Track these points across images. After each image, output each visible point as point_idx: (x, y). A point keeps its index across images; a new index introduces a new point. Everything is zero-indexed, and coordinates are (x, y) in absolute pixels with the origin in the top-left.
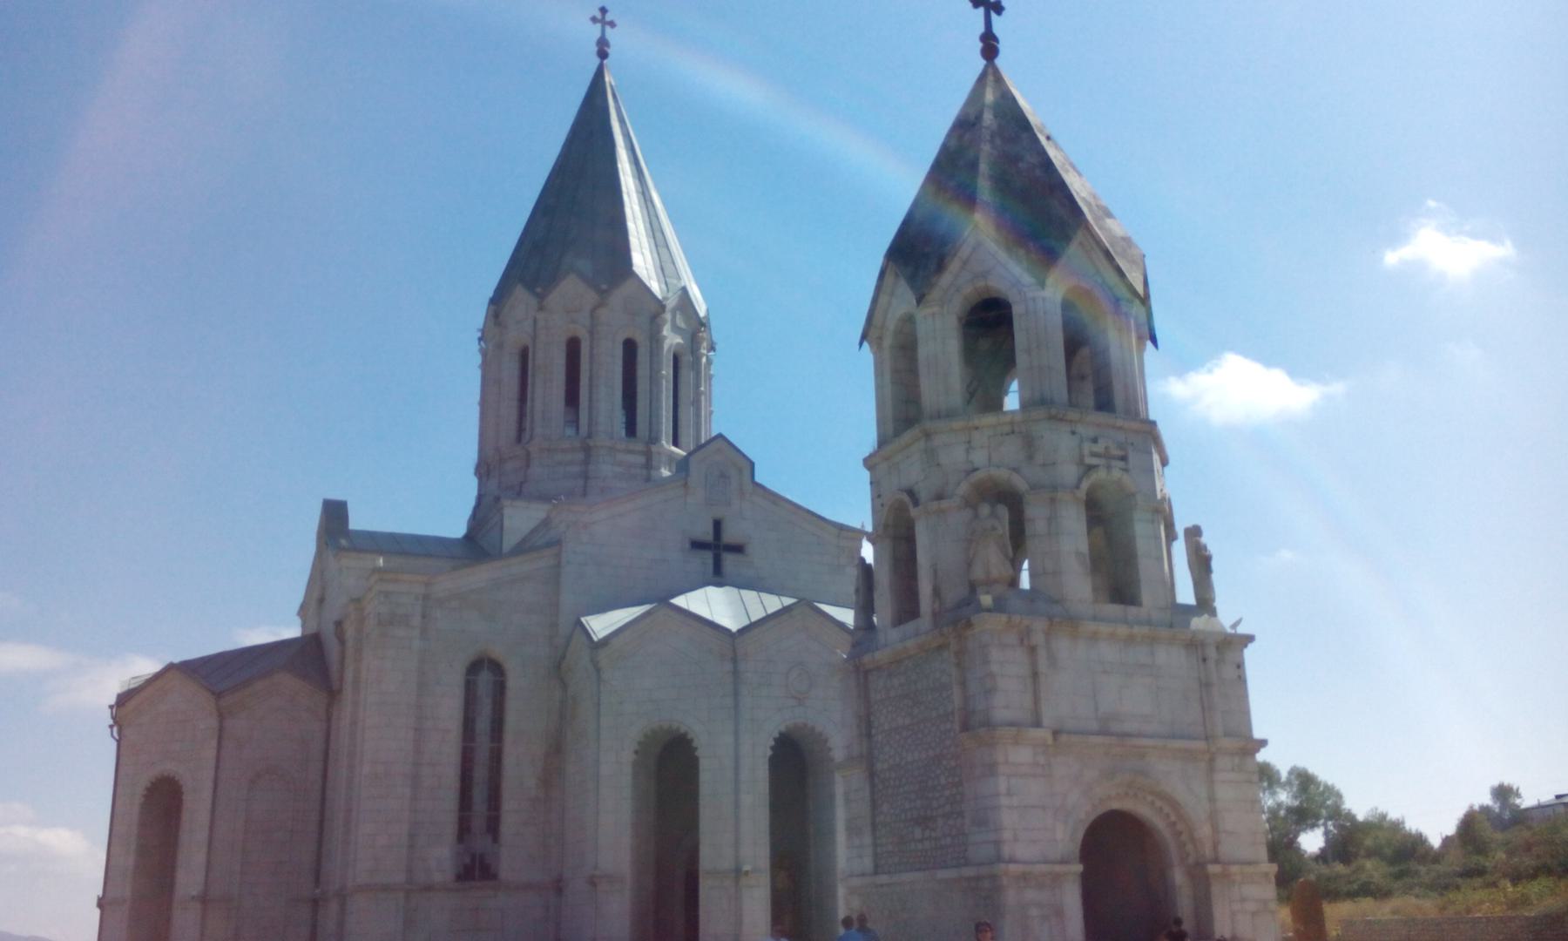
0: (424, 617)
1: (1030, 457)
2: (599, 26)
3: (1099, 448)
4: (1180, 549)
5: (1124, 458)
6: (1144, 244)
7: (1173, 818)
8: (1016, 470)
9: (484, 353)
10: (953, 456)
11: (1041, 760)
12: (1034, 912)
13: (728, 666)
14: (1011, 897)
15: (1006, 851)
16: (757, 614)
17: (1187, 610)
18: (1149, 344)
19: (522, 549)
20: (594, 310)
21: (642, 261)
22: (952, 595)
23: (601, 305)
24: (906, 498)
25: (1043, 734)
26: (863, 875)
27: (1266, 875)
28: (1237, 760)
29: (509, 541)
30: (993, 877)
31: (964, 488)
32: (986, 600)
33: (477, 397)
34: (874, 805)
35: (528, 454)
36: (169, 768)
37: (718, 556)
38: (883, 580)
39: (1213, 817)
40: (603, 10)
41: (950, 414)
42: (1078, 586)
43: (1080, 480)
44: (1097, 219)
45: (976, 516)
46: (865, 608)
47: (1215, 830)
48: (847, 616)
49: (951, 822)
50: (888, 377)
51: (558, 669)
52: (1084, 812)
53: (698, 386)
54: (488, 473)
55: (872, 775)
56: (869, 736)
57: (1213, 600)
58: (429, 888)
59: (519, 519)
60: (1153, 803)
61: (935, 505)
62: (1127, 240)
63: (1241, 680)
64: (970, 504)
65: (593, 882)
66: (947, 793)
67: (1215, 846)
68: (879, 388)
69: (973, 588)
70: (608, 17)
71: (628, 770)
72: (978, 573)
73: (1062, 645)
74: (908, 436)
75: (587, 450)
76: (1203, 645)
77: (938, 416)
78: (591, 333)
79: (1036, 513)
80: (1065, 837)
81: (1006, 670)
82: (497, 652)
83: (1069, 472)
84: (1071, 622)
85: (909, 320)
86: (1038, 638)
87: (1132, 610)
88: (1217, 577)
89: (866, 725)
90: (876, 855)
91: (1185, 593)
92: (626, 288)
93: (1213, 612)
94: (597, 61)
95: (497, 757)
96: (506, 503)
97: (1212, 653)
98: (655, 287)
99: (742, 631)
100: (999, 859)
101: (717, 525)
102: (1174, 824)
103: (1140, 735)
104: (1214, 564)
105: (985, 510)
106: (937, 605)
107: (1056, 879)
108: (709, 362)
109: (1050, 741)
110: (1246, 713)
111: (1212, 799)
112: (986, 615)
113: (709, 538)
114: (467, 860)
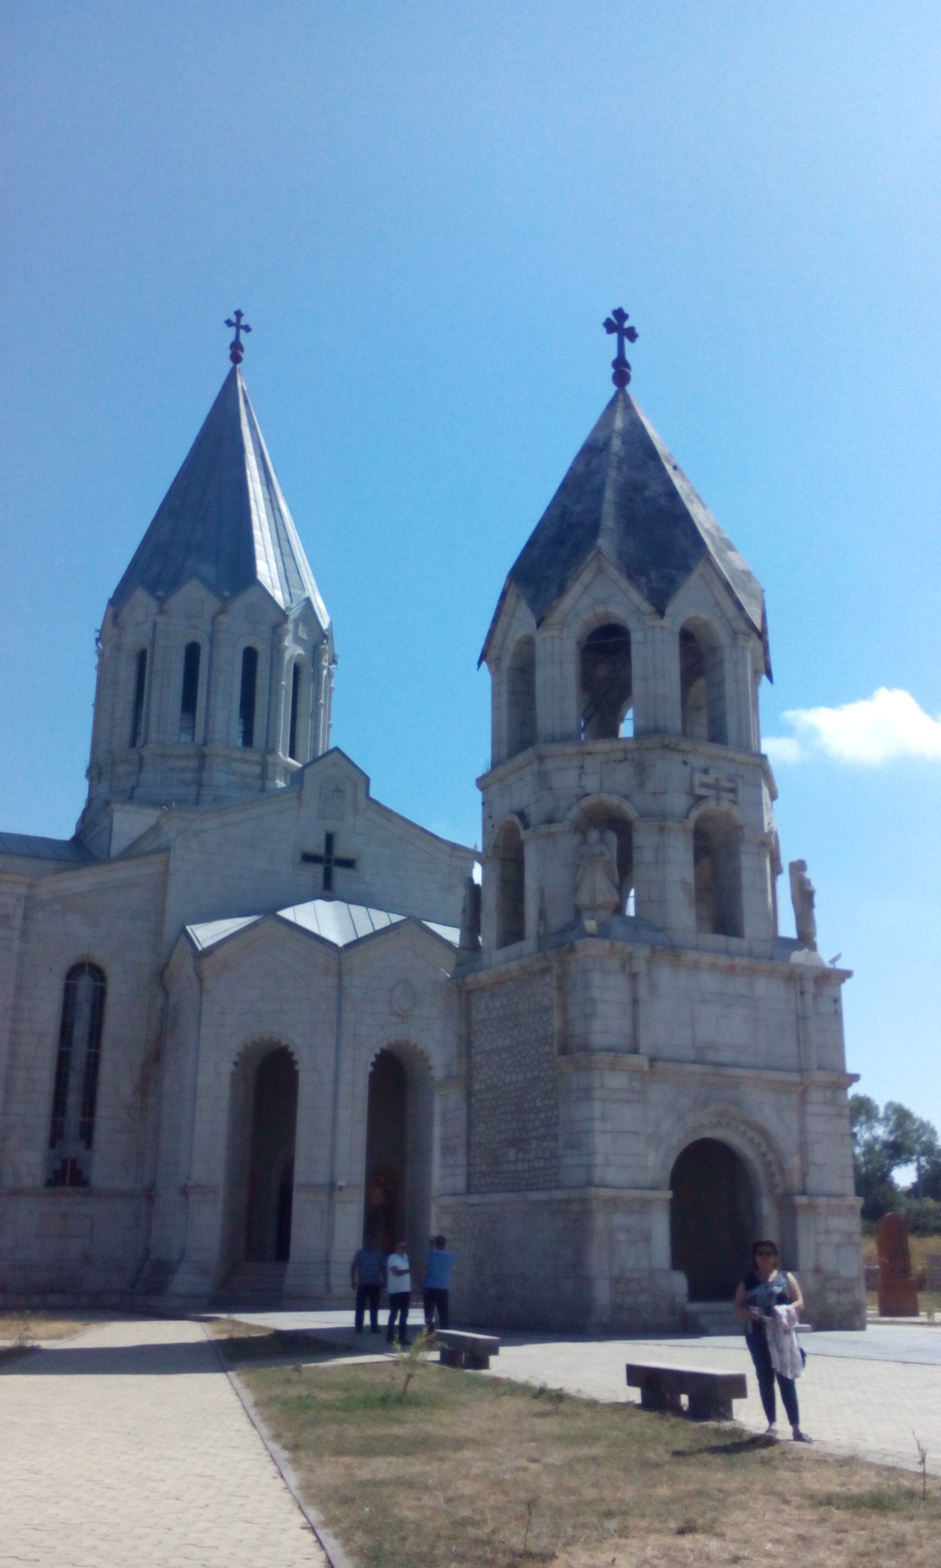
0: (25, 918)
1: (641, 785)
2: (233, 329)
3: (709, 779)
4: (784, 884)
5: (733, 791)
6: (765, 577)
7: (763, 1148)
8: (626, 797)
9: (101, 654)
10: (566, 780)
11: (637, 1086)
12: (622, 1236)
14: (600, 1221)
15: (598, 1175)
16: (364, 930)
17: (789, 944)
18: (764, 678)
19: (128, 854)
20: (214, 618)
21: (267, 569)
22: (558, 918)
23: (223, 611)
24: (516, 820)
25: (640, 1061)
26: (455, 1194)
27: (852, 1208)
28: (829, 1094)
29: (118, 846)
30: (584, 1201)
31: (573, 814)
32: (590, 925)
33: (91, 698)
34: (470, 1125)
37: (329, 870)
38: (490, 901)
39: (803, 1148)
40: (239, 314)
41: (566, 738)
42: (682, 915)
43: (689, 810)
44: (719, 551)
45: (585, 841)
46: (472, 928)
47: (805, 1162)
48: (453, 935)
49: (545, 1144)
50: (504, 698)
51: (161, 977)
52: (677, 1139)
53: (317, 699)
54: (100, 776)
55: (469, 1094)
56: (469, 1056)
57: (814, 935)
58: (17, 1192)
59: (128, 824)
60: (744, 1133)
61: (545, 829)
62: (747, 574)
63: (837, 1014)
64: (581, 828)
65: (185, 1191)
66: (543, 1115)
67: (804, 1176)
68: (496, 708)
69: (578, 912)
70: (243, 322)
71: (226, 1080)
72: (584, 898)
73: (664, 974)
74: (521, 758)
75: (202, 758)
76: (801, 978)
77: (553, 740)
78: (212, 640)
79: (644, 840)
80: (656, 1163)
81: (607, 996)
83: (677, 802)
84: (673, 950)
85: (528, 642)
86: (640, 966)
87: (734, 942)
88: (820, 913)
89: (466, 1045)
90: (469, 1176)
91: (787, 928)
92: (248, 597)
93: (813, 947)
94: (230, 364)
95: (93, 1063)
96: (116, 806)
97: (810, 987)
98: (279, 596)
99: (348, 946)
100: (590, 1183)
101: (330, 839)
102: (764, 1155)
103: (735, 1065)
104: (817, 900)
105: (594, 835)
106: (542, 930)
107: (645, 1205)
108: (330, 674)
109: (646, 1068)
110: (839, 1047)
111: (803, 1131)
112: (589, 939)
113: (321, 851)
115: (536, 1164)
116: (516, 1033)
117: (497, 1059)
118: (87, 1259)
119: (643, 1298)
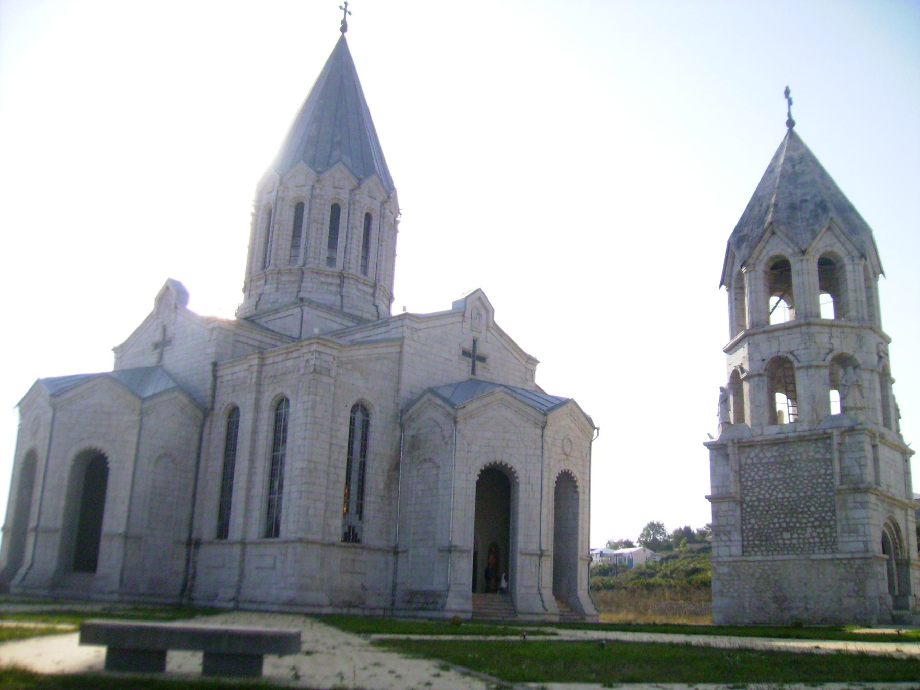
1: (861, 347)
13: (539, 432)
20: (352, 190)
35: (303, 273)
36: (99, 444)
40: (346, 3)
49: (819, 530)
55: (741, 503)
58: (333, 544)
66: (817, 515)
71: (473, 486)
82: (369, 398)
90: (743, 546)
95: (363, 466)
101: (475, 342)
111: (907, 529)
114: (346, 529)
115: (811, 540)
116: (788, 471)
117: (768, 484)
118: (364, 587)
119: (884, 607)
